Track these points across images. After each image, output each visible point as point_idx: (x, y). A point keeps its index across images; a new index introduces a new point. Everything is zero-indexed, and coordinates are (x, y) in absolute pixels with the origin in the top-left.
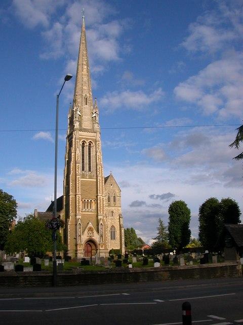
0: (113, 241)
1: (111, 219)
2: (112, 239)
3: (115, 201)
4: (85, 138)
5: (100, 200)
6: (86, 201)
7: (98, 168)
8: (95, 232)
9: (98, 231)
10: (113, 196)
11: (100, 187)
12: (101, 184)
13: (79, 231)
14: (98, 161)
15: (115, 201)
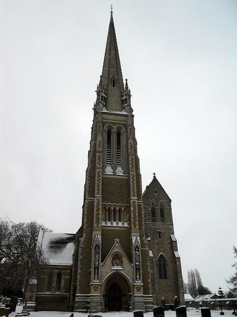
0: (164, 282)
1: (158, 244)
2: (161, 278)
3: (162, 215)
4: (110, 123)
5: (134, 207)
6: (112, 209)
7: (130, 159)
8: (125, 261)
9: (131, 261)
10: (159, 207)
11: (134, 186)
12: (135, 182)
13: (95, 258)
14: (129, 150)
15: (162, 215)
